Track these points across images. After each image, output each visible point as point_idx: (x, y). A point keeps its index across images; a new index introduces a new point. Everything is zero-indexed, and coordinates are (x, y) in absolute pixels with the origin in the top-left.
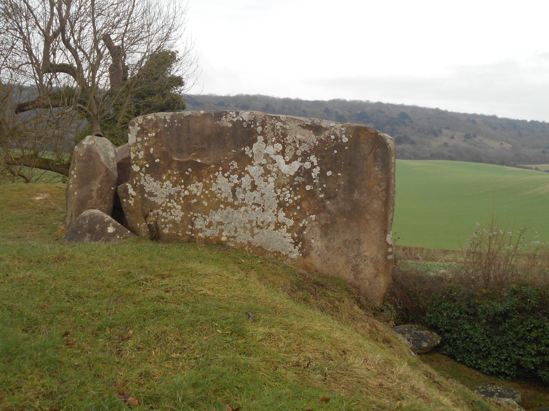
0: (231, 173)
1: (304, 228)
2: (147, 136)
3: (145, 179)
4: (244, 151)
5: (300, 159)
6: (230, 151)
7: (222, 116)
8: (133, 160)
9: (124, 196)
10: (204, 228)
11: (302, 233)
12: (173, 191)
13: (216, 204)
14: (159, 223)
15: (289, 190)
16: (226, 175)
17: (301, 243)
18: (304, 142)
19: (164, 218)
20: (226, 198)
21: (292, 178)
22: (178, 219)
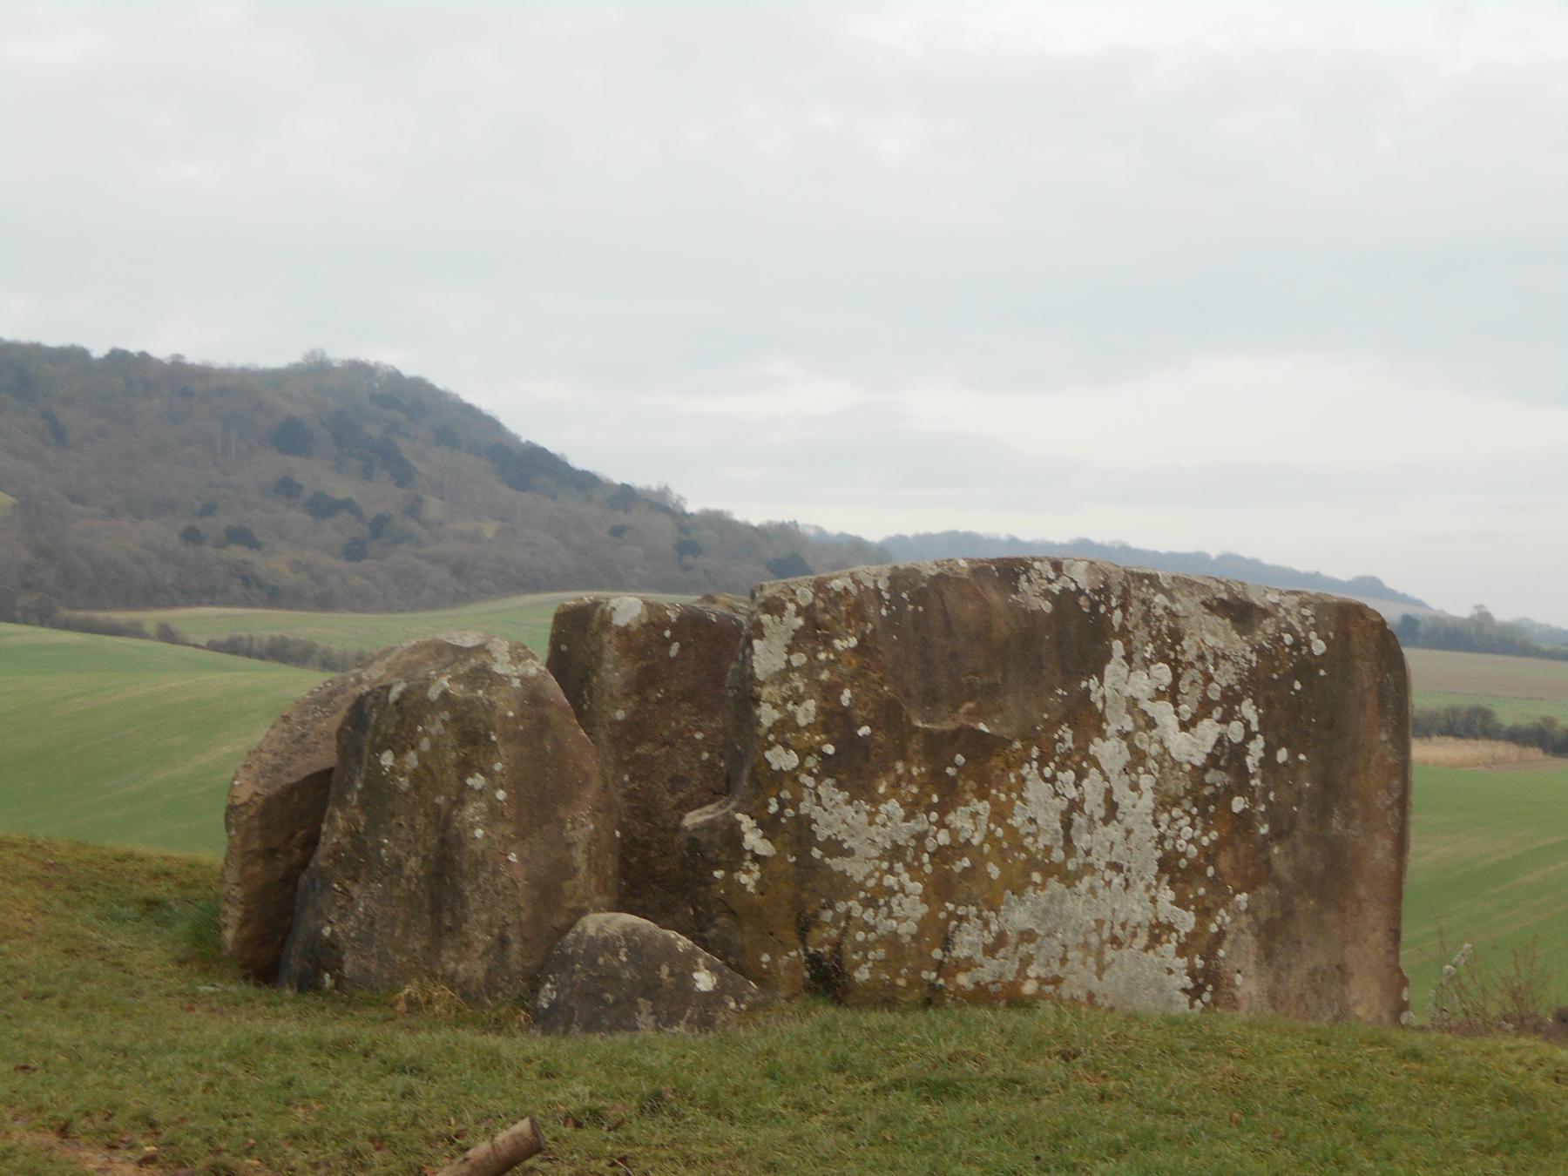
0: (1057, 769)
1: (1220, 936)
2: (828, 646)
3: (818, 797)
4: (1088, 691)
5: (1217, 713)
6: (1052, 691)
7: (1017, 577)
8: (770, 730)
9: (724, 857)
10: (979, 957)
11: (1215, 954)
12: (903, 832)
13: (1030, 869)
14: (847, 946)
15: (1188, 813)
16: (1048, 772)
17: (1210, 988)
18: (1225, 657)
19: (870, 928)
20: (1048, 850)
21: (1199, 772)
22: (907, 929)
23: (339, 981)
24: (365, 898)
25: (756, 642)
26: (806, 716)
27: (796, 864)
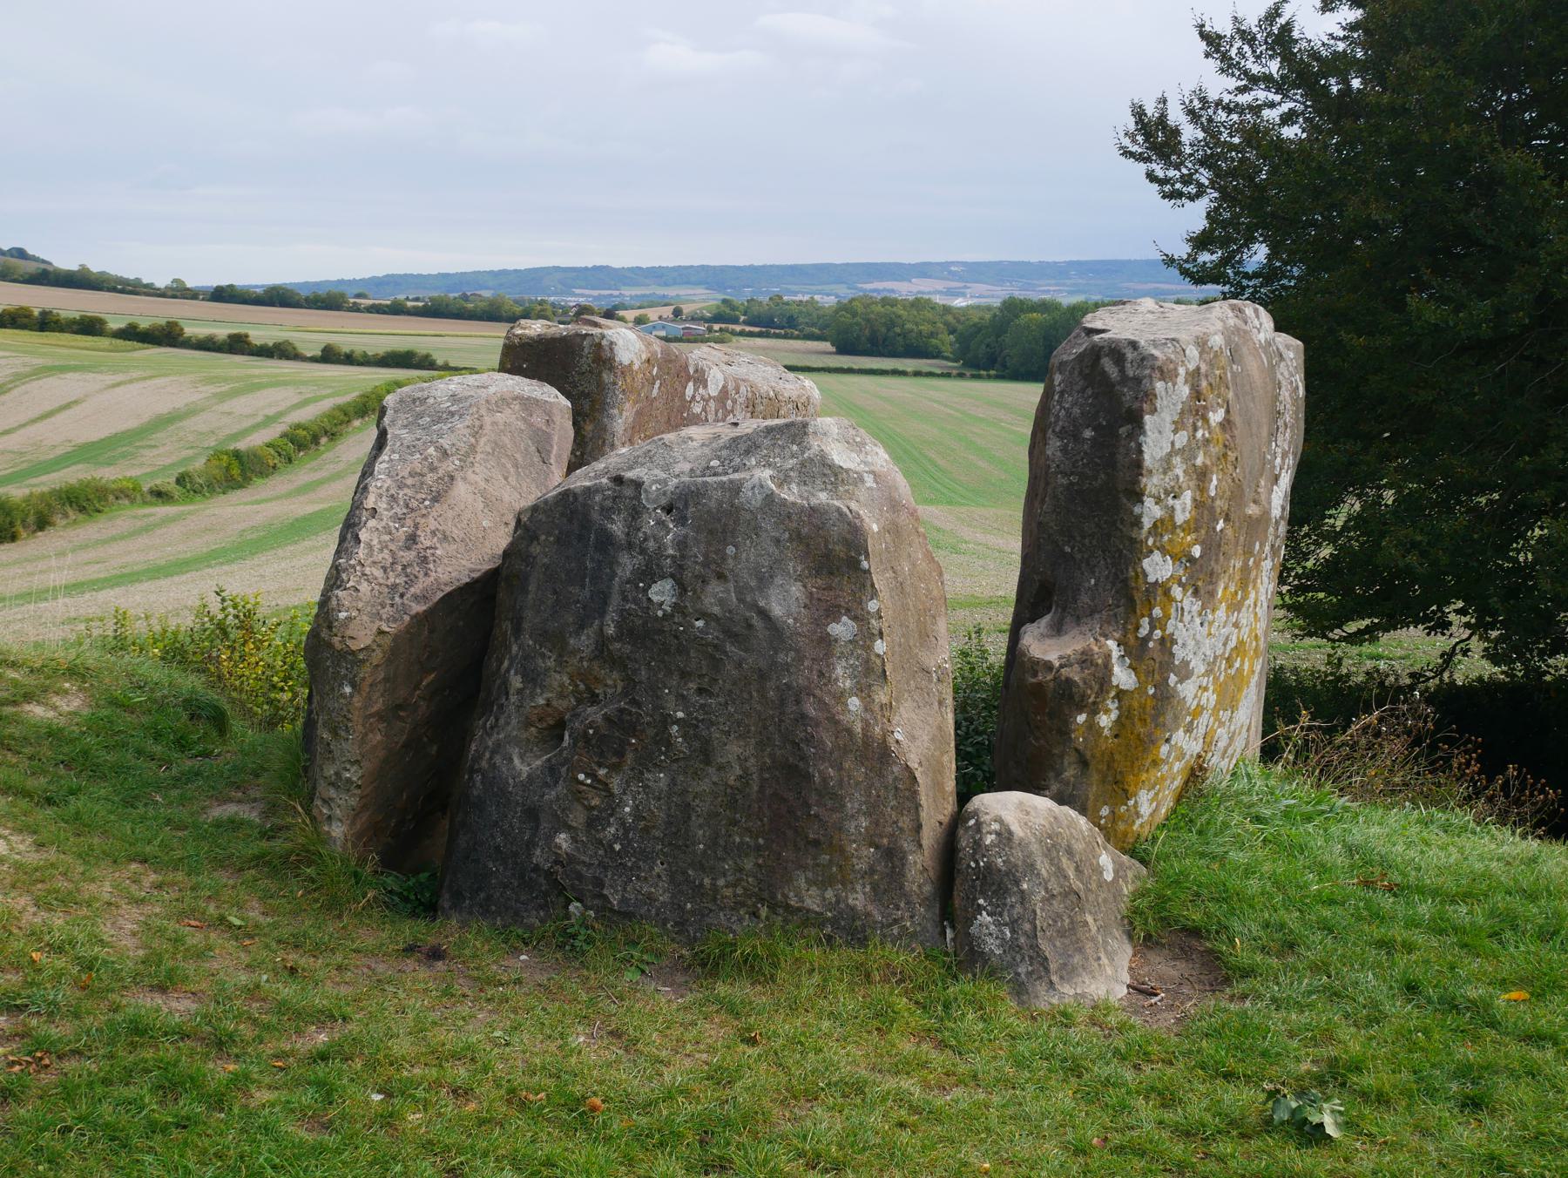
25: (1147, 418)
26: (1184, 510)
27: (1154, 696)
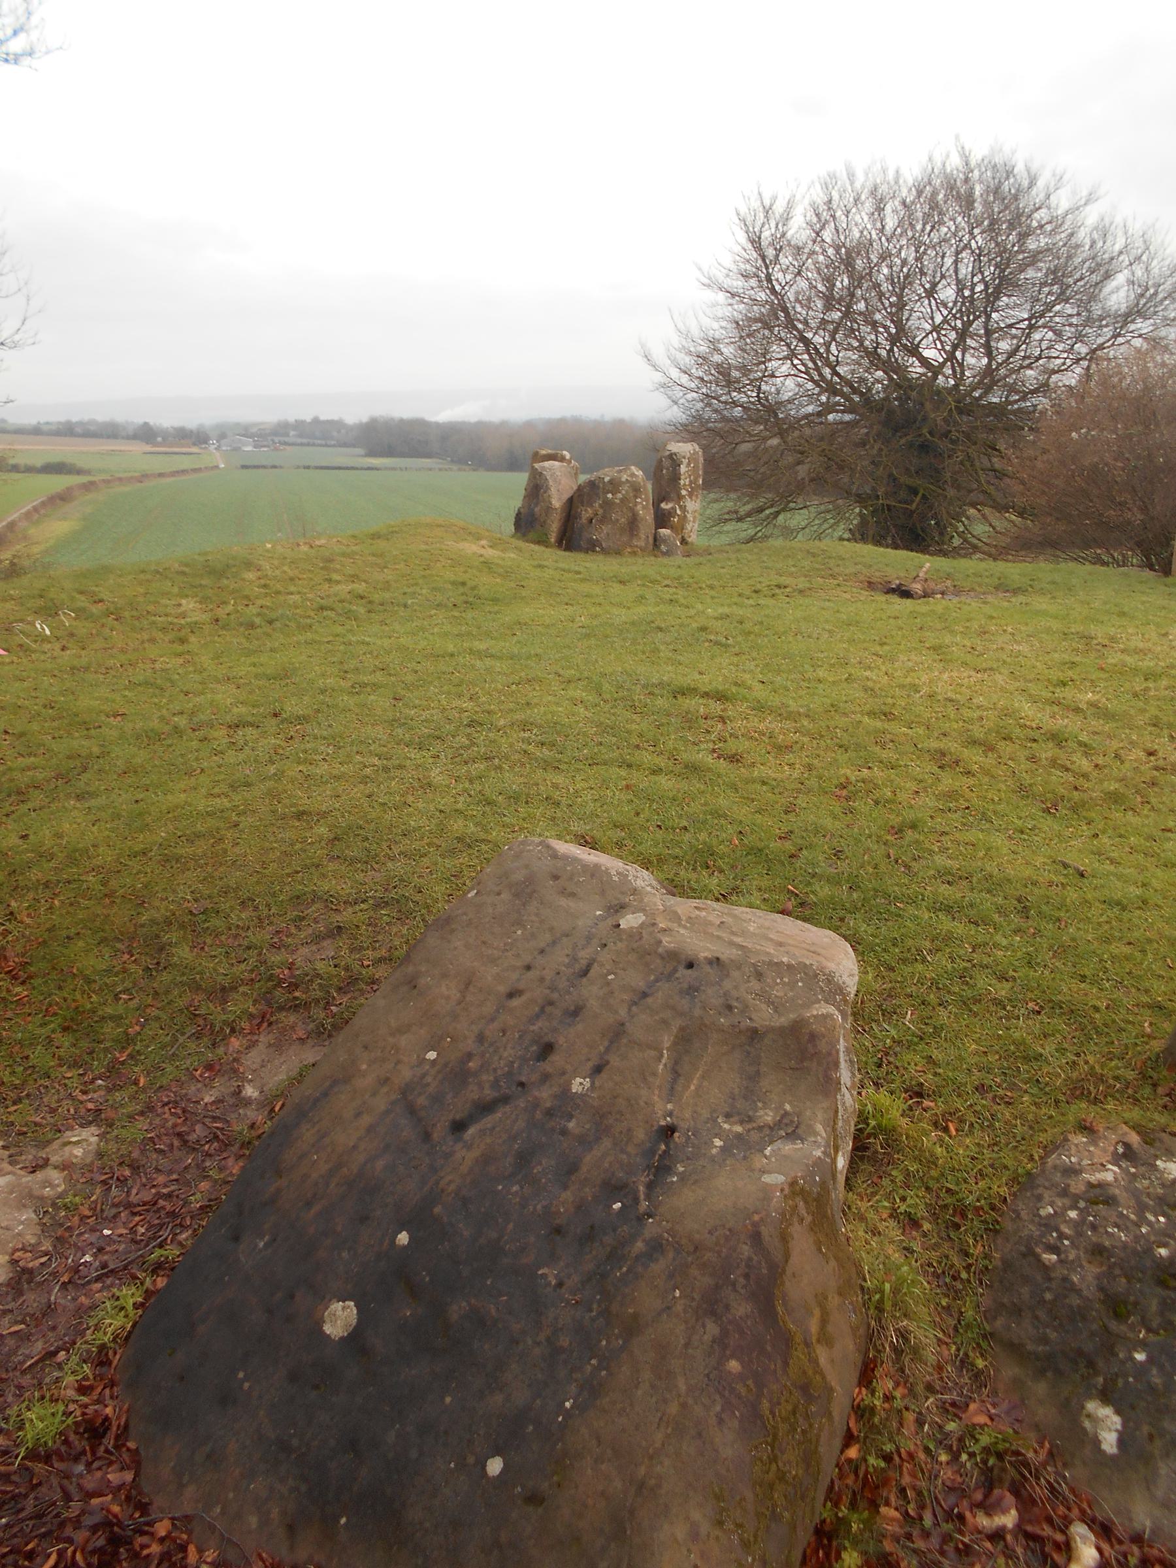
23: (602, 549)
24: (606, 529)
